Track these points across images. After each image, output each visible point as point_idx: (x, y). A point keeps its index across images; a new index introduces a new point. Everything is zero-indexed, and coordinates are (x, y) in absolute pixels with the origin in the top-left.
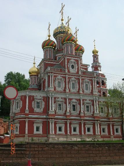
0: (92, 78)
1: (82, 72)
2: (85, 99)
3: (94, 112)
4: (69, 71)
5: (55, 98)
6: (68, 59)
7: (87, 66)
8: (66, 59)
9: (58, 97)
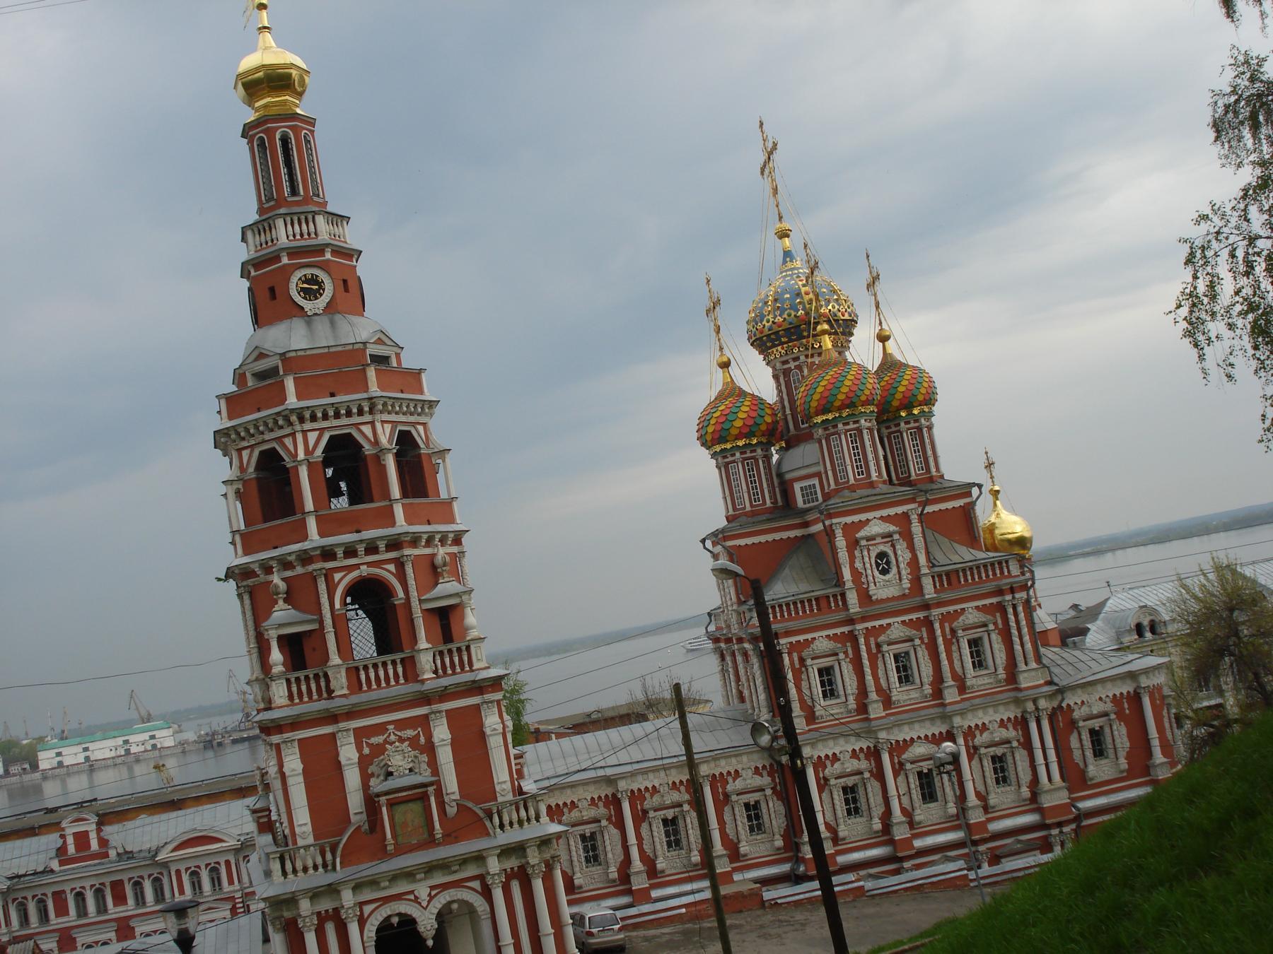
0: (1000, 592)
1: (940, 576)
2: (977, 725)
3: (1035, 780)
4: (865, 597)
6: (850, 530)
7: (969, 494)
8: (839, 533)
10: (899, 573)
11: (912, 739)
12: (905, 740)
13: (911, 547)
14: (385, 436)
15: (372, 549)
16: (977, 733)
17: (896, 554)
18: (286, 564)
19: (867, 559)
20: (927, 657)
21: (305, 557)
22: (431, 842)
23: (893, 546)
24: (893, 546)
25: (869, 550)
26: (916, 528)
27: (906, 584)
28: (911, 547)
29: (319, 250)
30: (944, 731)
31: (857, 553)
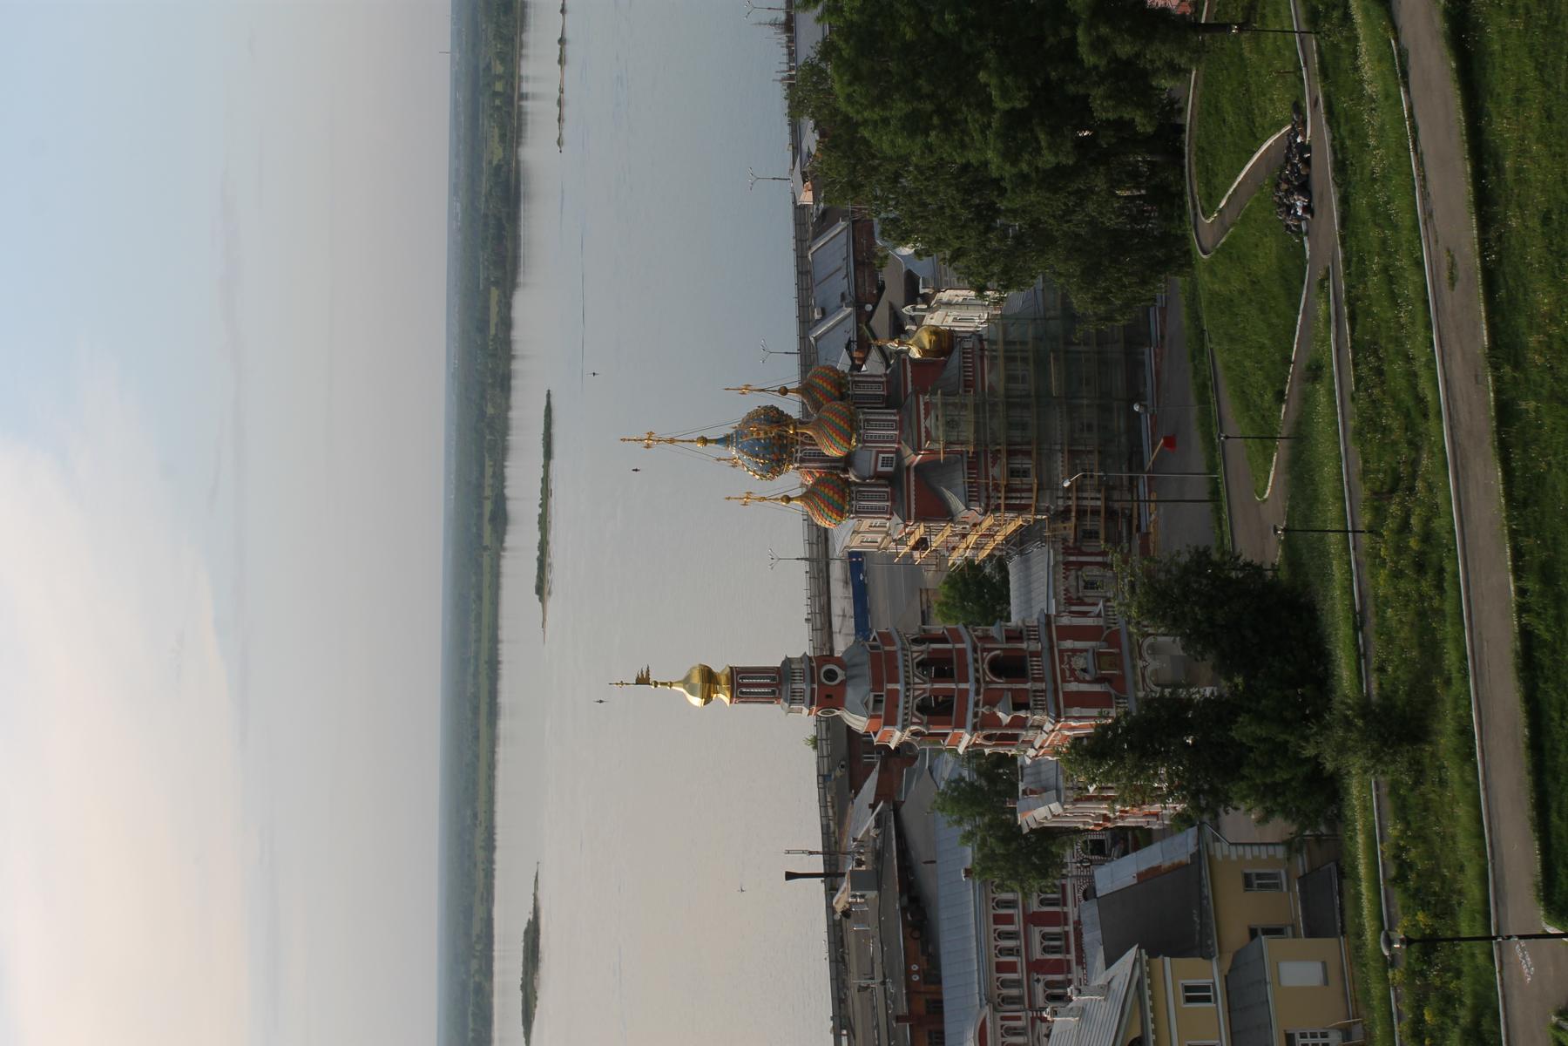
0: (982, 358)
14: (915, 648)
15: (976, 660)
18: (976, 704)
21: (977, 693)
22: (1120, 654)
29: (812, 668)
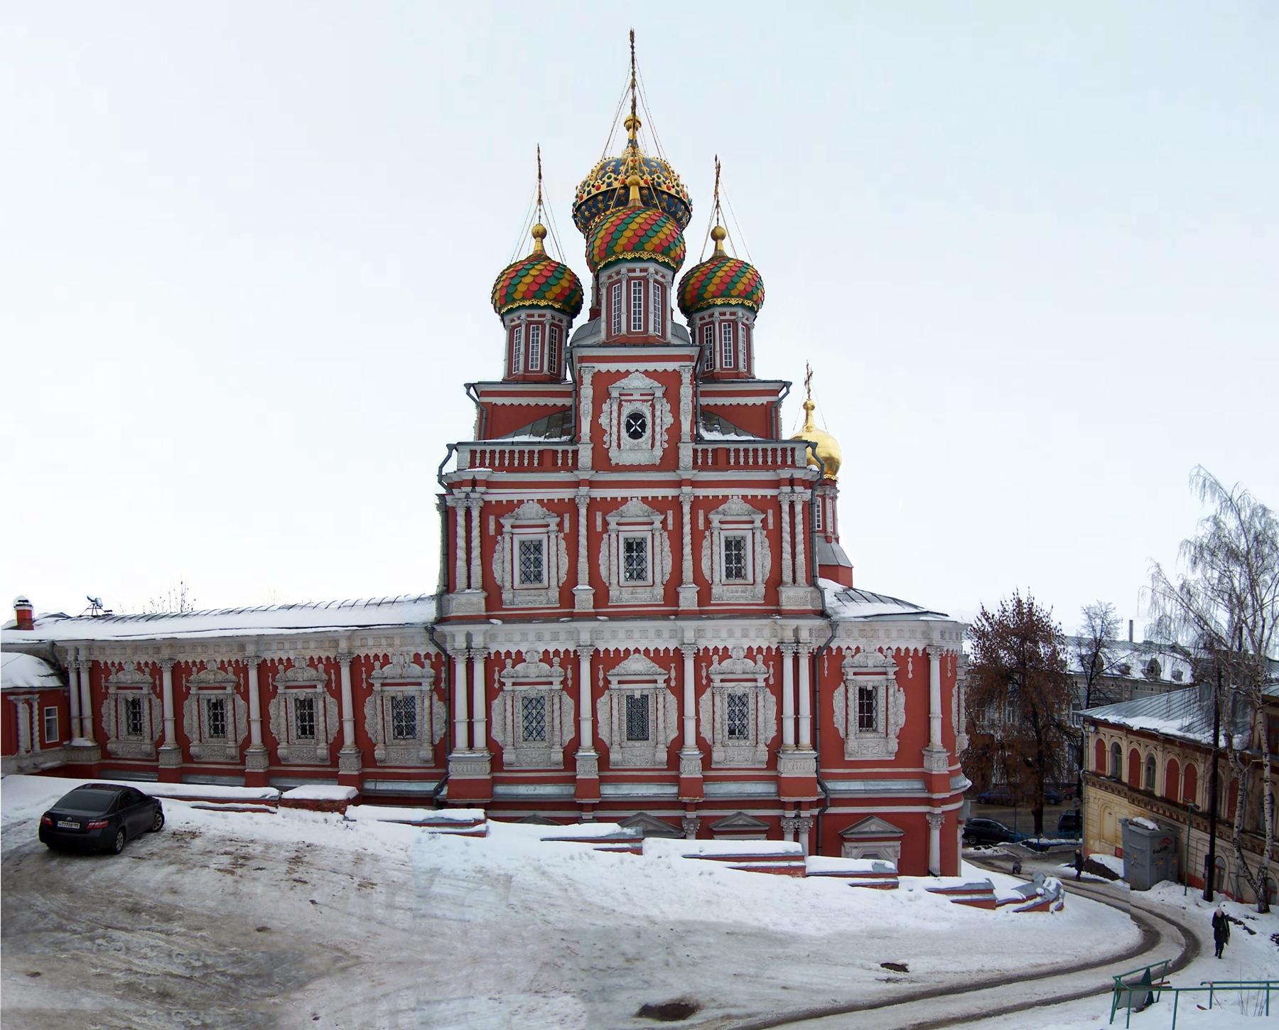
2: (716, 649)
4: (601, 460)
5: (494, 663)
6: (597, 376)
9: (519, 653)
10: (653, 439)
11: (627, 650)
12: (617, 650)
13: (676, 412)
16: (716, 658)
17: (653, 416)
19: (615, 414)
20: (667, 549)
23: (653, 406)
24: (653, 406)
25: (620, 406)
26: (686, 391)
27: (658, 452)
28: (676, 412)
30: (672, 648)
31: (605, 407)
